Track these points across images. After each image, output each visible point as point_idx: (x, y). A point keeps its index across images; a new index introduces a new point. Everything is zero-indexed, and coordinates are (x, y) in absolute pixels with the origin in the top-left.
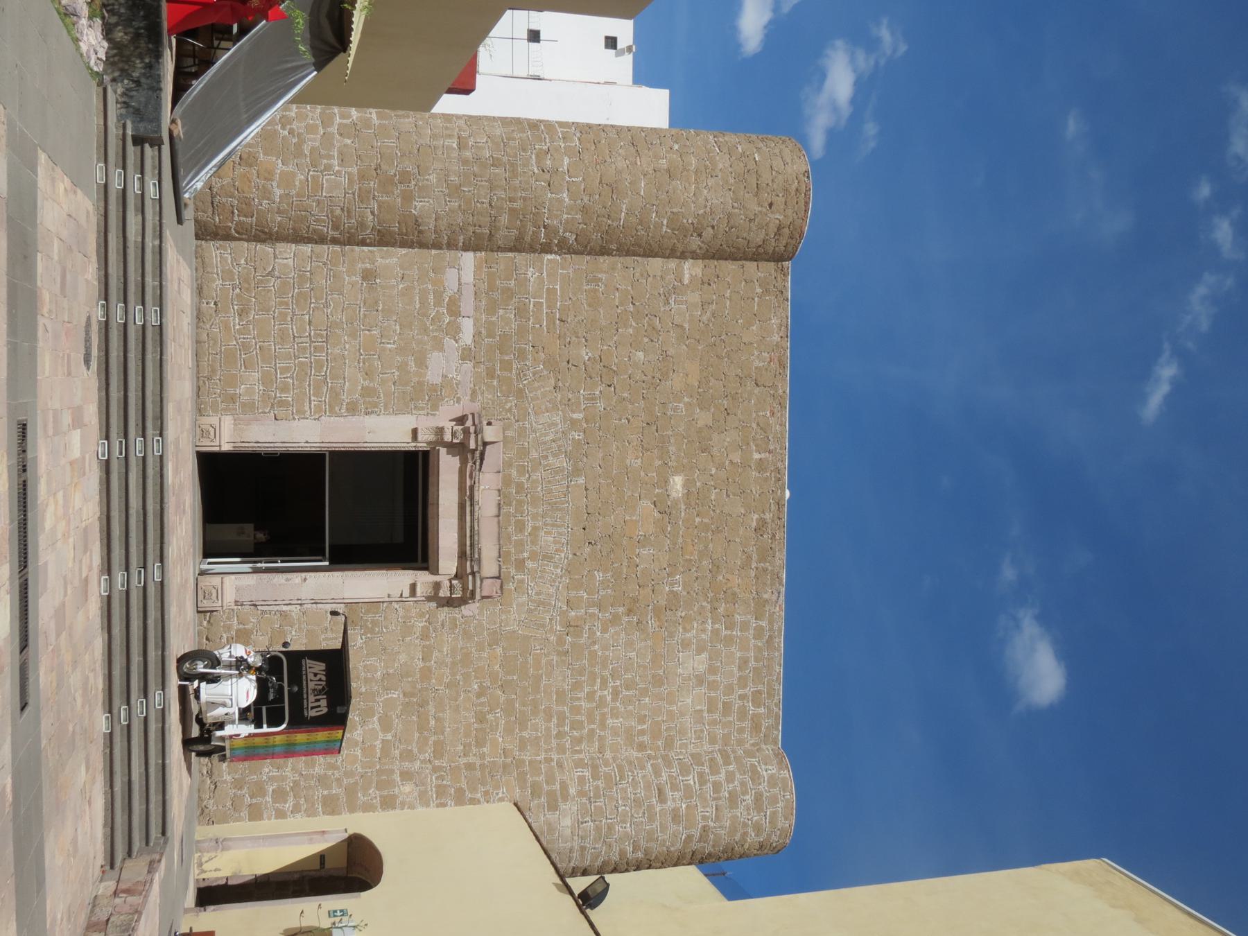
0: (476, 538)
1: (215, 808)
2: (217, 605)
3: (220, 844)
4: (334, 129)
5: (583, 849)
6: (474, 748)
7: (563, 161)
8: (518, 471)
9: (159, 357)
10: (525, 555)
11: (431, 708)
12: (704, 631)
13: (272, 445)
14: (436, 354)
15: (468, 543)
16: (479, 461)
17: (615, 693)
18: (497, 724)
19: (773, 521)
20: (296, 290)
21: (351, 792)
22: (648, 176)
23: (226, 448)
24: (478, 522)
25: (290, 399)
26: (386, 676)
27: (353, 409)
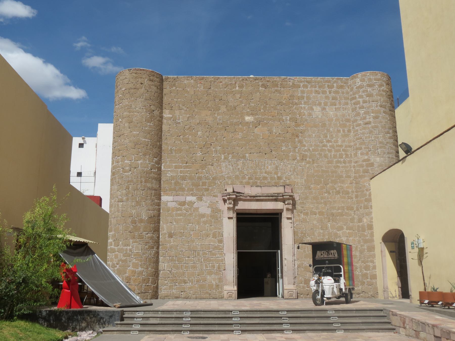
0: (269, 195)
1: (372, 292)
2: (295, 292)
3: (385, 290)
4: (116, 248)
5: (388, 153)
6: (350, 195)
7: (126, 163)
8: (244, 179)
9: (202, 312)
10: (276, 176)
11: (334, 211)
12: (304, 108)
13: (235, 271)
14: (200, 210)
15: (271, 198)
16: (240, 194)
17: (328, 141)
18: (340, 186)
19: (262, 82)
20: (176, 262)
21: (366, 241)
22: (132, 130)
23: (236, 288)
24: (263, 194)
25: (217, 265)
26: (322, 228)
27: (221, 241)
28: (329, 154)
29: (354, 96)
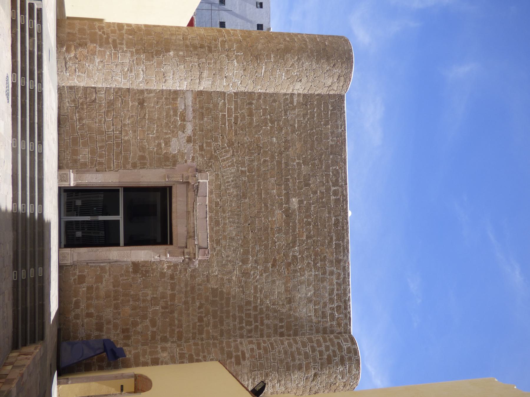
11: (176, 315)
18: (209, 323)
25: (104, 161)
26: (153, 299)
27: (134, 166)
28: (251, 308)
29: (328, 340)
